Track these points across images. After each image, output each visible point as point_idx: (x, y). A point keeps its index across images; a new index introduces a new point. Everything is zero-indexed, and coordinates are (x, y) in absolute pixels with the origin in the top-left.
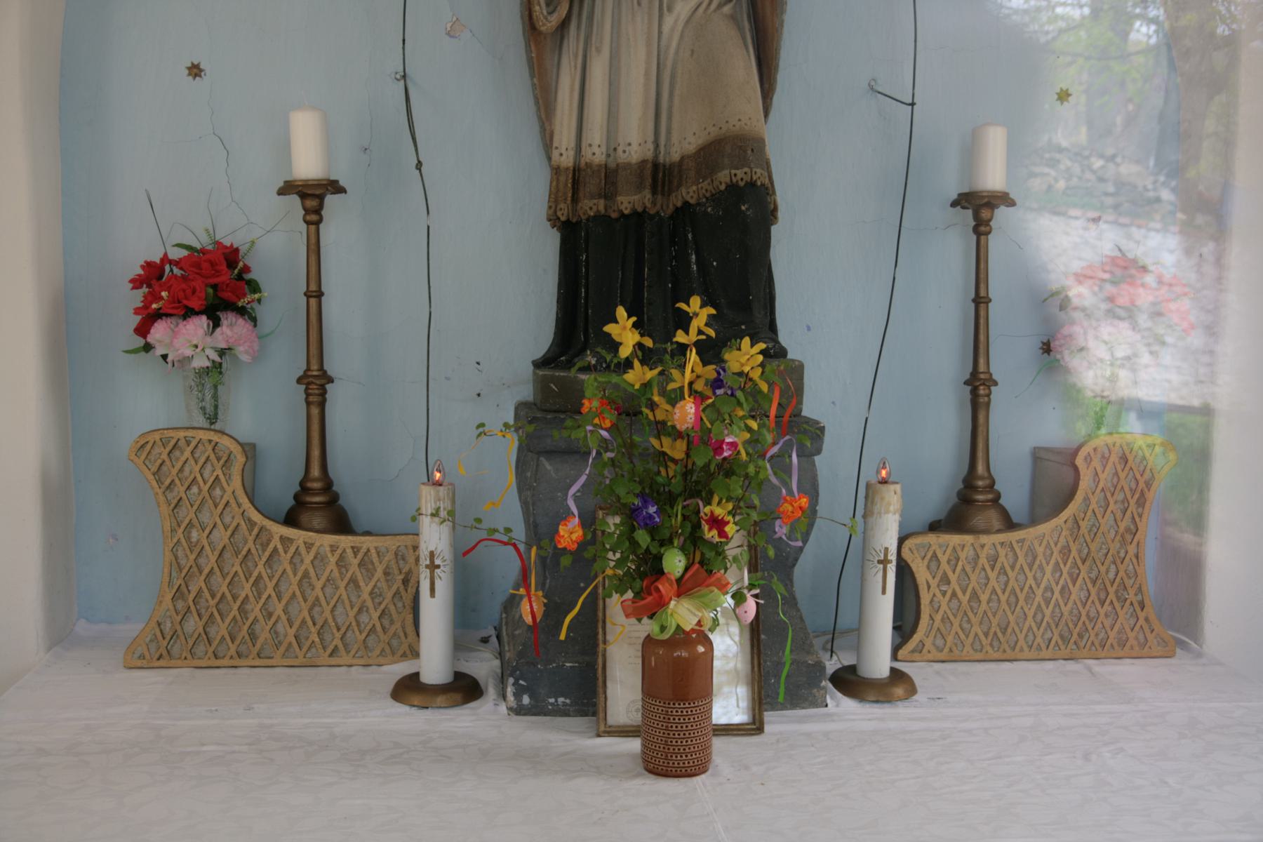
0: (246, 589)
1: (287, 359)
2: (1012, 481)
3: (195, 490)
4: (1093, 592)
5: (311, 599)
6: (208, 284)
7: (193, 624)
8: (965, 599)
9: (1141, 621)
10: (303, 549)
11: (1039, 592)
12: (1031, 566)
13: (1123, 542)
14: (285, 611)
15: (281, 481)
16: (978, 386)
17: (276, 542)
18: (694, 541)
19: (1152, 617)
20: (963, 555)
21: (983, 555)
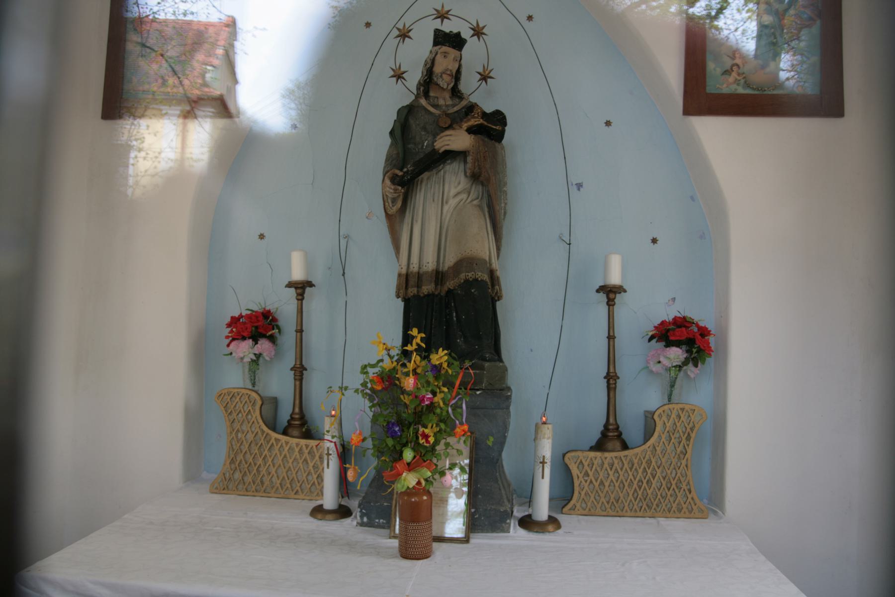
0: (260, 461)
1: (290, 360)
2: (632, 429)
3: (240, 415)
4: (664, 483)
5: (287, 468)
6: (257, 327)
7: (238, 475)
8: (597, 484)
9: (690, 499)
10: (284, 445)
11: (635, 483)
12: (631, 469)
13: (679, 458)
14: (276, 472)
15: (285, 415)
16: (611, 379)
17: (273, 441)
18: (417, 448)
19: (695, 498)
20: (596, 462)
21: (606, 463)
